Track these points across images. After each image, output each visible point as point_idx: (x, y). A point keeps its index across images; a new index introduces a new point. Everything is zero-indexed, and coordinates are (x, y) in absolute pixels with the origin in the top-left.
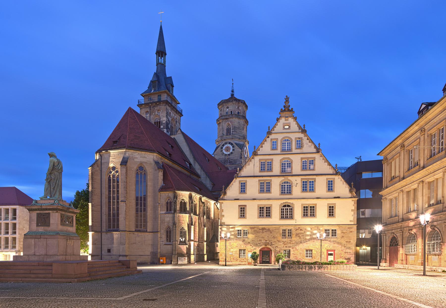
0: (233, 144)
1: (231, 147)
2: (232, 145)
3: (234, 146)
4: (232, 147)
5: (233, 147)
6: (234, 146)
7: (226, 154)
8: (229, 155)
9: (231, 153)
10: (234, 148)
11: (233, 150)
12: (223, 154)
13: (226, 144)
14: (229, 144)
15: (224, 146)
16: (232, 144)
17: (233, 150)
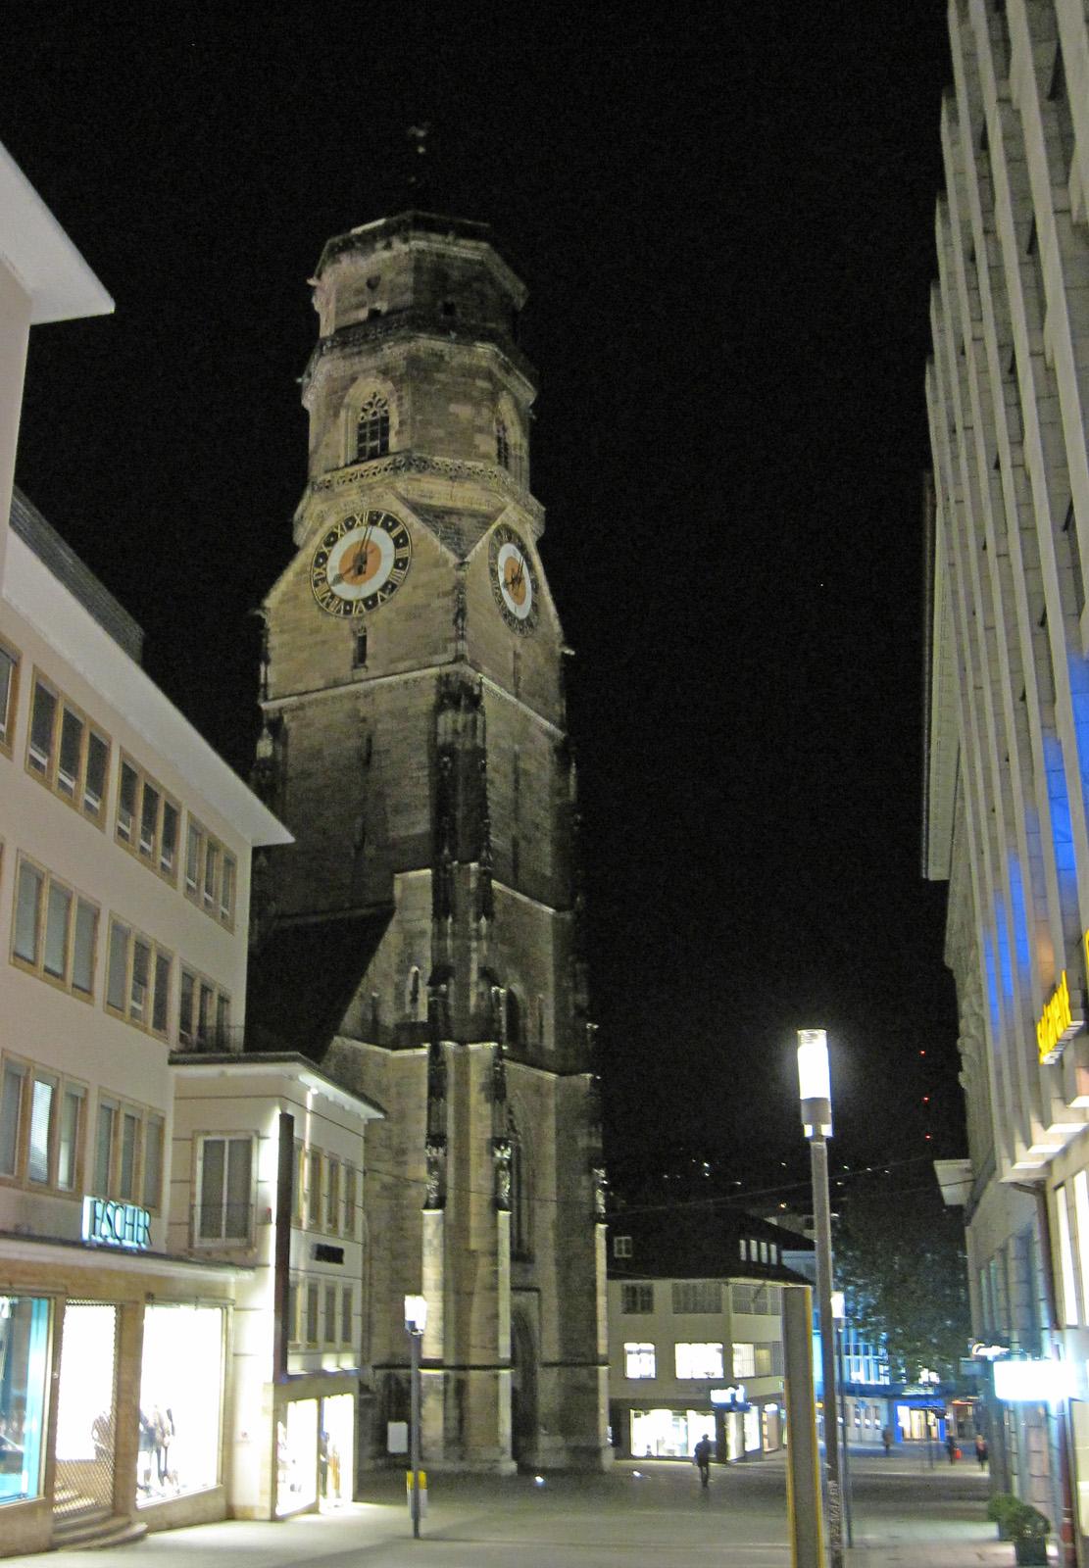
0: (396, 523)
1: (382, 538)
2: (389, 530)
3: (403, 534)
4: (391, 544)
5: (396, 541)
6: (403, 534)
7: (349, 603)
8: (371, 602)
9: (383, 589)
10: (405, 552)
11: (401, 564)
12: (328, 605)
13: (350, 528)
14: (373, 522)
15: (336, 541)
16: (391, 523)
17: (396, 566)
